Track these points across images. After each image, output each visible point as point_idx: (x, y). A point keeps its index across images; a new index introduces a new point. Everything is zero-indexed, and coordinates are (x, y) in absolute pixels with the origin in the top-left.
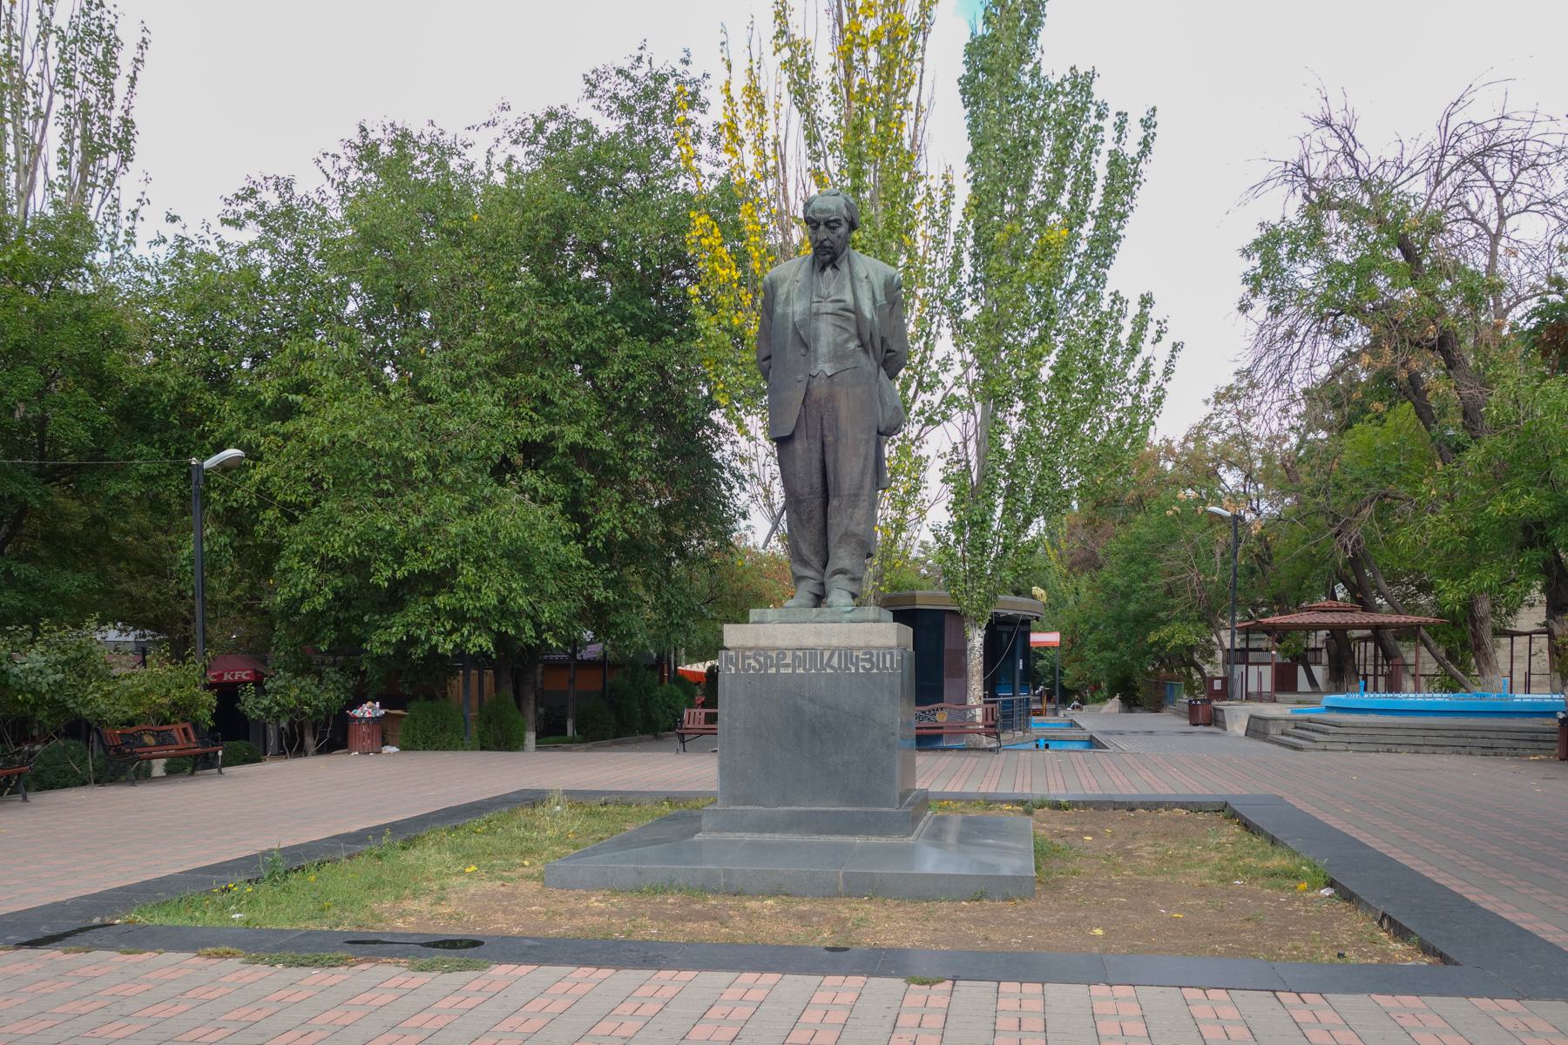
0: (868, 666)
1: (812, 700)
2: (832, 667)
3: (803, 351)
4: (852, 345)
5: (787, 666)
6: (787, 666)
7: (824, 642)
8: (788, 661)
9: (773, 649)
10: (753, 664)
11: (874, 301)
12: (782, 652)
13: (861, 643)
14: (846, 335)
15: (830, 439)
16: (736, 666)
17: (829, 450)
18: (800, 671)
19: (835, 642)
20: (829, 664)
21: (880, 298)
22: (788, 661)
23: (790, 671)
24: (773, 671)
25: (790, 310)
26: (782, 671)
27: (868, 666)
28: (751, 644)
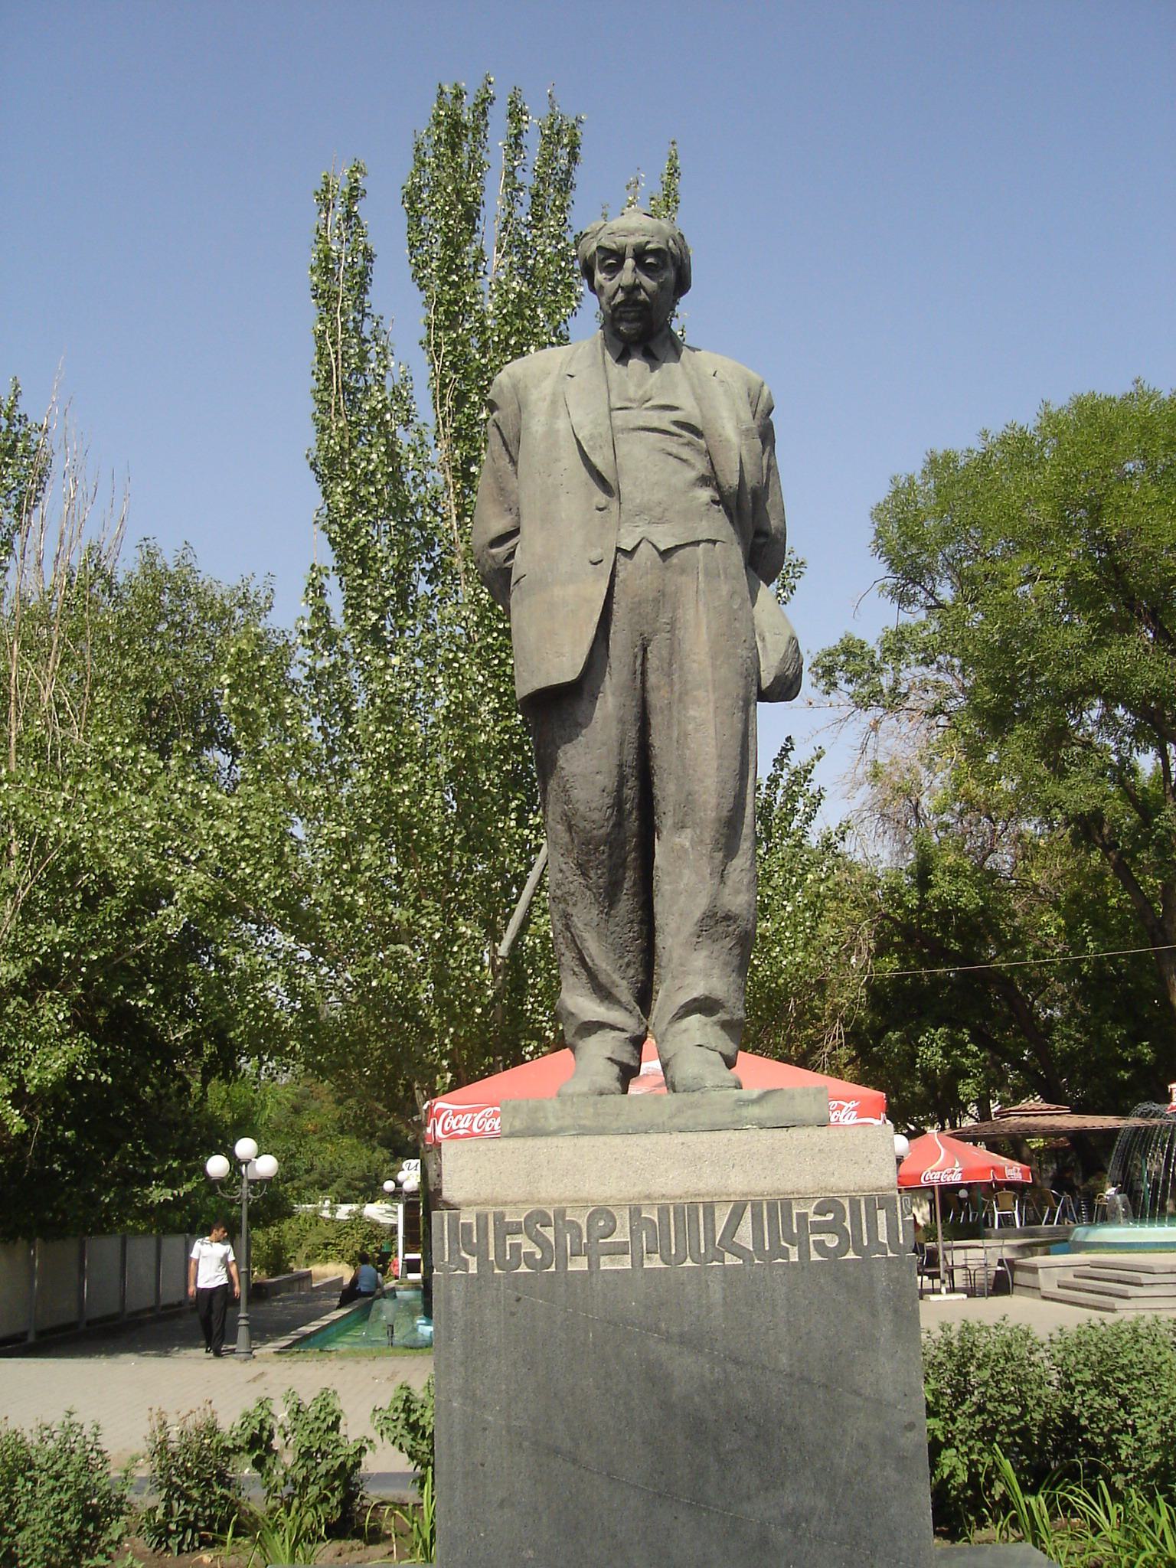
0: (832, 1241)
1: (689, 1342)
2: (739, 1251)
3: (600, 498)
4: (706, 494)
5: (620, 1250)
6: (620, 1250)
7: (705, 1182)
8: (622, 1236)
9: (580, 1203)
10: (528, 1246)
11: (739, 420)
12: (602, 1213)
13: (805, 1182)
14: (692, 475)
16: (481, 1254)
17: (656, 720)
18: (655, 1262)
19: (738, 1183)
20: (728, 1242)
21: (746, 414)
22: (622, 1236)
23: (625, 1263)
24: (579, 1265)
25: (562, 425)
26: (606, 1264)
27: (832, 1241)
28: (516, 1192)
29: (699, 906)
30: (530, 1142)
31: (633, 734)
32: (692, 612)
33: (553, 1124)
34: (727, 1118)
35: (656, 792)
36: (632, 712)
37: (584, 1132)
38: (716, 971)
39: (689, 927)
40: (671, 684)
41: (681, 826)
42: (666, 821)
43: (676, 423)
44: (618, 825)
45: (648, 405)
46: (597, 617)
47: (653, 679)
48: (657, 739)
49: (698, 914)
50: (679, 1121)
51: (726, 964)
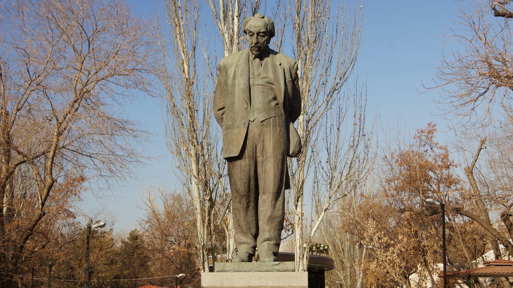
15: (259, 160)
17: (259, 165)
29: (269, 214)
30: (222, 273)
31: (253, 169)
32: (268, 137)
33: (228, 269)
34: (270, 269)
35: (259, 184)
36: (252, 163)
37: (236, 271)
38: (273, 231)
39: (266, 220)
40: (263, 156)
41: (264, 193)
42: (261, 191)
43: (267, 83)
44: (249, 191)
45: (260, 77)
46: (243, 139)
47: (258, 154)
48: (259, 170)
49: (268, 216)
50: (259, 269)
51: (275, 229)
